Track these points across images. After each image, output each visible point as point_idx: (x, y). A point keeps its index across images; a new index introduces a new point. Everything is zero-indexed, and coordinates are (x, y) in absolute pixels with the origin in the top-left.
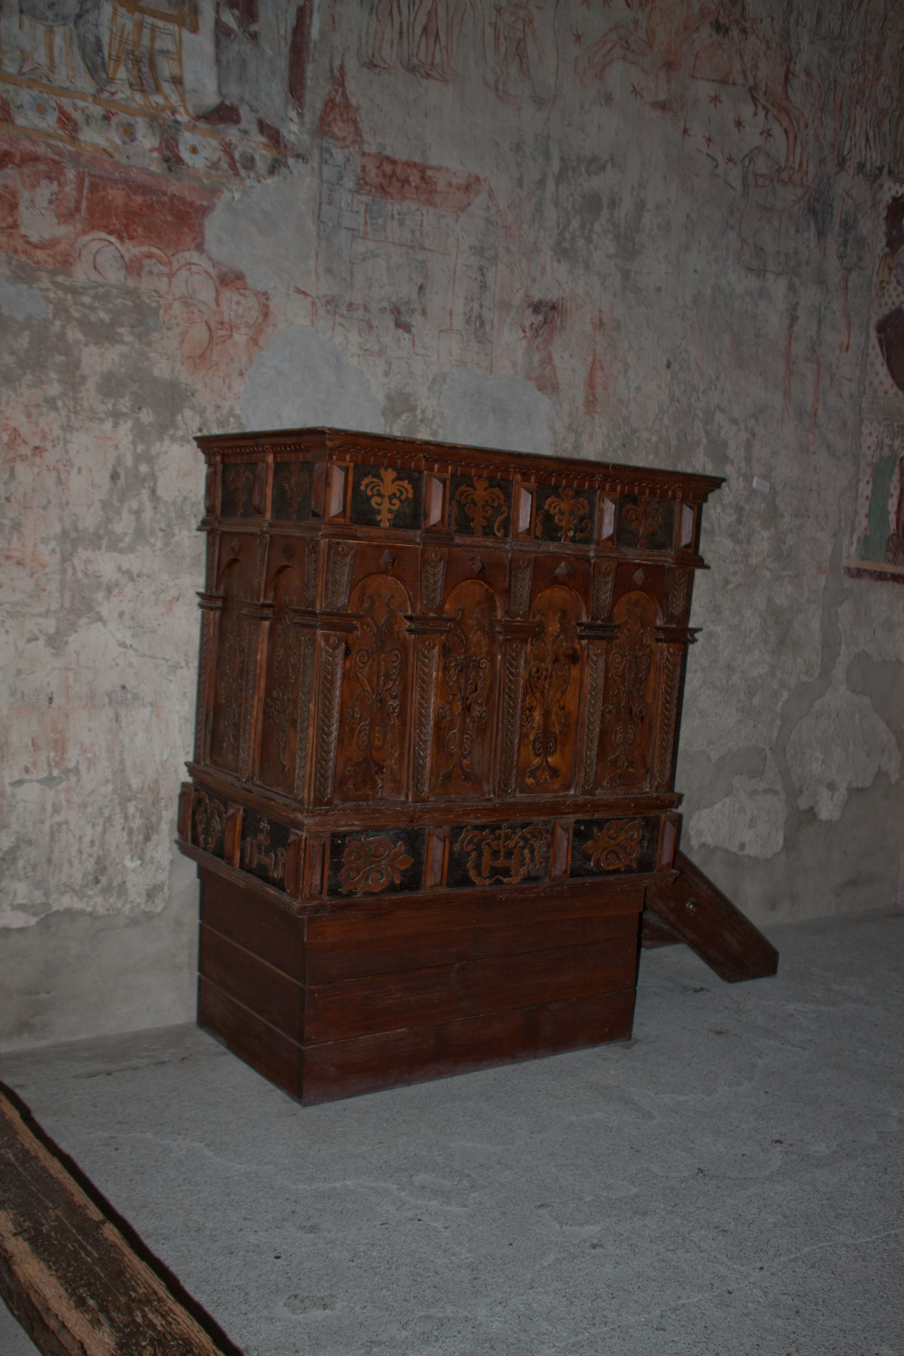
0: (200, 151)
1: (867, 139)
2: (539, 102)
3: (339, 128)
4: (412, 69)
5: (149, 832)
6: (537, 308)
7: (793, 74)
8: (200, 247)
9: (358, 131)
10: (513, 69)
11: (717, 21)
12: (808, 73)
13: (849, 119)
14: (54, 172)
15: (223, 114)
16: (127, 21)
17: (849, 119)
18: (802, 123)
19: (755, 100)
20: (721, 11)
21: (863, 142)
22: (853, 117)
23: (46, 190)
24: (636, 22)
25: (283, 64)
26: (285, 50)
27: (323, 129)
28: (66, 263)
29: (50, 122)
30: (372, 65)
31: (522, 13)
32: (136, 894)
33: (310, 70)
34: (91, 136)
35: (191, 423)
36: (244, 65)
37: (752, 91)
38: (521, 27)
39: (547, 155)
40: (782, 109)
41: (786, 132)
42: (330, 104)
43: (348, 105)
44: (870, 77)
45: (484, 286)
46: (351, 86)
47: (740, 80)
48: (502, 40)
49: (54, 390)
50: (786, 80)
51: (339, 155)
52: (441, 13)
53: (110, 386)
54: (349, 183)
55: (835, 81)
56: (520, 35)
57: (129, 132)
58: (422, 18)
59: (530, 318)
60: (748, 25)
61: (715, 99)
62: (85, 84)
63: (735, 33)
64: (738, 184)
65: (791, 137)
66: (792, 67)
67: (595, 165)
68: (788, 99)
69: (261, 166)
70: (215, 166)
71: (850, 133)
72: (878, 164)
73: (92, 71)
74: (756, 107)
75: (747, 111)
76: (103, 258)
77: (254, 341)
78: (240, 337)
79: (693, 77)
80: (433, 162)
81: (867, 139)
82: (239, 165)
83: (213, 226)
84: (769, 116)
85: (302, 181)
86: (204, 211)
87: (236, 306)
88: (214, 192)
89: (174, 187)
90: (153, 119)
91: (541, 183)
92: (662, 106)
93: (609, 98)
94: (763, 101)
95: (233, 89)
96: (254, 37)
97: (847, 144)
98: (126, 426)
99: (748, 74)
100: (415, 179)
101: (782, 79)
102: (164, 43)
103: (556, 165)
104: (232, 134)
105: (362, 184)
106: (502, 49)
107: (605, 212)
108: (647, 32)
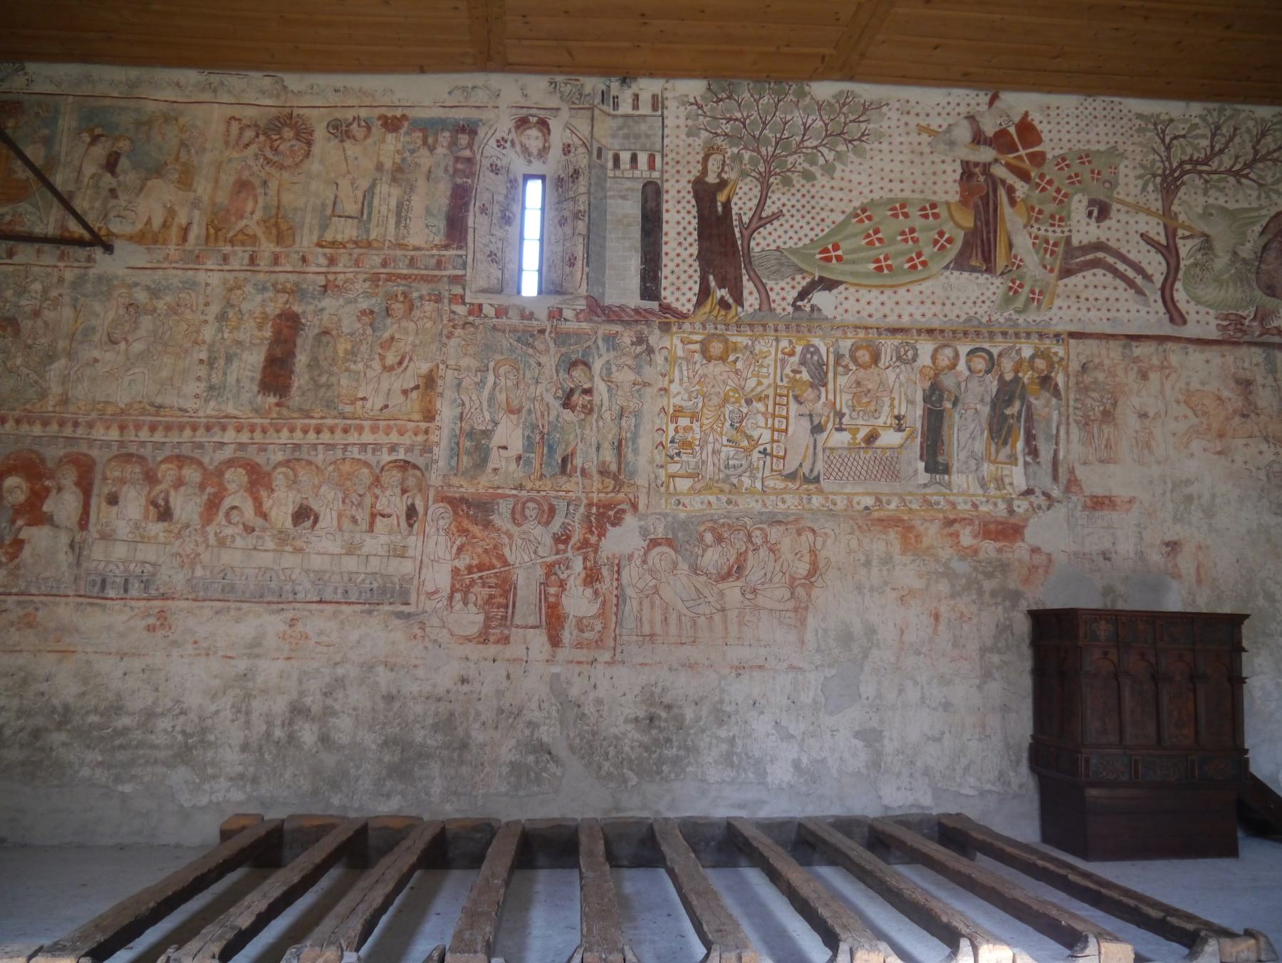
0: (1021, 506)
2: (1159, 463)
3: (1074, 489)
4: (1102, 462)
5: (1018, 761)
6: (1167, 544)
8: (1023, 540)
9: (1081, 489)
10: (1146, 452)
14: (971, 522)
15: (1029, 492)
16: (993, 468)
19: (1268, 442)
23: (968, 529)
25: (1050, 470)
26: (1050, 465)
27: (1067, 490)
28: (976, 552)
29: (969, 506)
30: (1085, 463)
32: (1015, 787)
33: (1060, 470)
34: (983, 508)
35: (1024, 605)
36: (1035, 473)
37: (1266, 439)
39: (1165, 483)
42: (1069, 481)
43: (1076, 480)
45: (1141, 539)
46: (1077, 473)
49: (974, 597)
51: (1074, 498)
53: (994, 594)
54: (1079, 508)
57: (995, 504)
59: (1165, 549)
61: (1246, 445)
62: (980, 491)
63: (1253, 416)
64: (1264, 478)
67: (1188, 482)
69: (1044, 507)
70: (1027, 511)
73: (982, 487)
75: (1264, 447)
76: (989, 548)
77: (1046, 572)
78: (1041, 571)
80: (1114, 493)
82: (1036, 509)
83: (1028, 532)
85: (1060, 511)
86: (1024, 527)
87: (1037, 559)
88: (1027, 520)
89: (1012, 520)
90: (1003, 499)
91: (1164, 494)
92: (1219, 453)
93: (1192, 455)
95: (1032, 483)
96: (1038, 463)
98: (1000, 609)
100: (1107, 502)
102: (1006, 472)
103: (1170, 486)
104: (1032, 498)
105: (1085, 507)
107: (1196, 502)
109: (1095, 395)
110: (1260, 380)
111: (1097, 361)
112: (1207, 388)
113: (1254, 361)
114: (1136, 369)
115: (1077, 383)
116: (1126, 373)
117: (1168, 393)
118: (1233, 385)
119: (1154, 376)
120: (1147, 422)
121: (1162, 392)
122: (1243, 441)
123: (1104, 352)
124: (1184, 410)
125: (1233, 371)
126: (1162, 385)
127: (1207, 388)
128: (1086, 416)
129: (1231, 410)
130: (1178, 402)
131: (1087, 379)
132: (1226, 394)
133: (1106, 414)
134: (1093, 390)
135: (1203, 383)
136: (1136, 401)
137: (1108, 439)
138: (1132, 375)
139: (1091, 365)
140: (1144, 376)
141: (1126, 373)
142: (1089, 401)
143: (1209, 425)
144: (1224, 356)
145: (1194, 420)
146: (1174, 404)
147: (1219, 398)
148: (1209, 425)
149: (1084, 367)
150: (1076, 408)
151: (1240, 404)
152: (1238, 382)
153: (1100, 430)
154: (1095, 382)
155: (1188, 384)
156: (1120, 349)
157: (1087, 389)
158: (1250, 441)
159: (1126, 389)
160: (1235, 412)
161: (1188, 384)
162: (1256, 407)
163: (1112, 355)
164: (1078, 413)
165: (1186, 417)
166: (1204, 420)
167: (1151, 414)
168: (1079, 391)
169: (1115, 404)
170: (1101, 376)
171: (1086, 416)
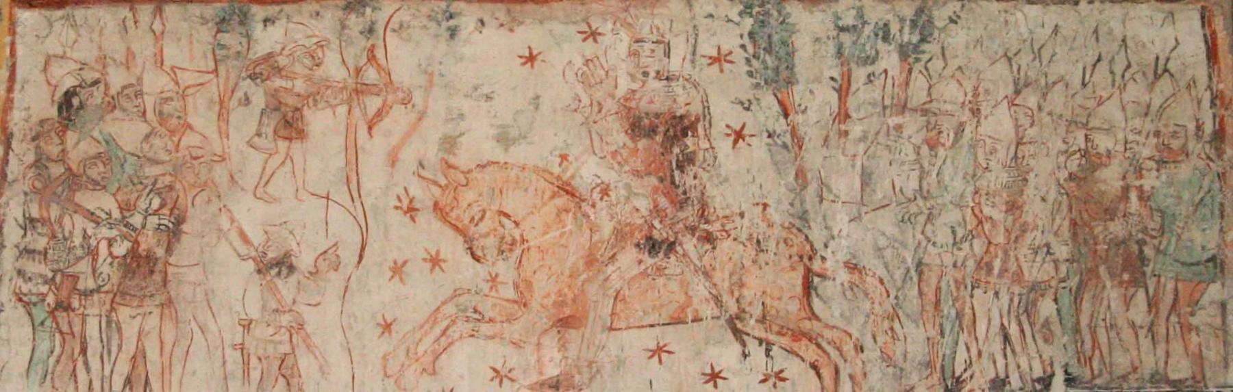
1: (1006, 338)
7: (822, 276)
11: (649, 238)
12: (853, 267)
13: (959, 315)
17: (959, 315)
18: (848, 348)
19: (738, 334)
20: (656, 223)
21: (997, 346)
22: (968, 311)
24: (493, 280)
31: (285, 319)
38: (287, 337)
40: (799, 335)
41: (814, 367)
44: (1000, 239)
47: (708, 310)
48: (254, 361)
50: (808, 287)
52: (153, 354)
55: (919, 264)
56: (286, 348)
58: (123, 368)
60: (715, 228)
61: (659, 351)
63: (689, 244)
65: (827, 373)
66: (816, 265)
68: (814, 316)
71: (963, 338)
72: (1038, 372)
74: (744, 344)
75: (726, 355)
79: (611, 329)
81: (1006, 338)
84: (775, 350)
94: (759, 332)
97: (962, 355)
99: (726, 298)
101: (799, 289)
106: (255, 375)
108: (516, 286)
109: (103, 202)
110: (724, 114)
111: (117, 78)
112: (520, 154)
113: (707, 48)
114: (259, 100)
115: (39, 163)
116: (223, 115)
117: (373, 176)
118: (619, 138)
119: (319, 121)
120: (286, 288)
121: (352, 180)
122: (649, 339)
123: (143, 46)
124: (431, 234)
125: (624, 84)
126: (352, 151)
127: (520, 154)
128: (64, 280)
129: (607, 228)
130: (411, 211)
131: (79, 147)
132: (589, 172)
133: (138, 264)
134: (99, 185)
135: (504, 139)
136: (250, 215)
137: (139, 357)
138: (244, 122)
139: (97, 97)
140: (290, 126)
141: (223, 115)
142: (77, 225)
143: (523, 289)
144: (594, 35)
145: (465, 271)
146: (397, 219)
147: (567, 189)
148: (523, 289)
149: (68, 105)
150: (27, 252)
151: (644, 204)
152: (637, 127)
153: (111, 323)
154: (107, 155)
155: (449, 143)
156: (205, 34)
157: (73, 180)
158: (671, 336)
159: (220, 174)
160: (620, 235)
161: (449, 143)
162: (703, 215)
163: (173, 54)
164: (34, 267)
165: (435, 261)
166: (505, 270)
167: (305, 261)
168: (43, 190)
169: (173, 233)
170: (128, 133)
171: (64, 280)
